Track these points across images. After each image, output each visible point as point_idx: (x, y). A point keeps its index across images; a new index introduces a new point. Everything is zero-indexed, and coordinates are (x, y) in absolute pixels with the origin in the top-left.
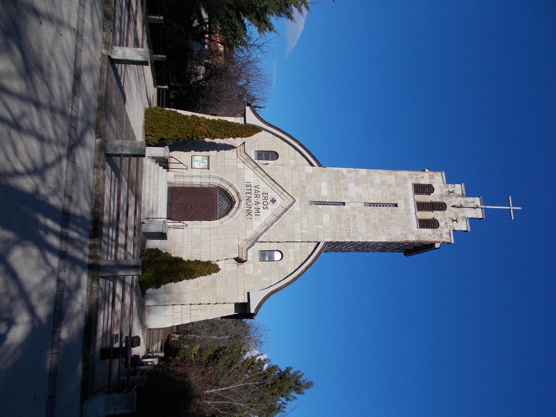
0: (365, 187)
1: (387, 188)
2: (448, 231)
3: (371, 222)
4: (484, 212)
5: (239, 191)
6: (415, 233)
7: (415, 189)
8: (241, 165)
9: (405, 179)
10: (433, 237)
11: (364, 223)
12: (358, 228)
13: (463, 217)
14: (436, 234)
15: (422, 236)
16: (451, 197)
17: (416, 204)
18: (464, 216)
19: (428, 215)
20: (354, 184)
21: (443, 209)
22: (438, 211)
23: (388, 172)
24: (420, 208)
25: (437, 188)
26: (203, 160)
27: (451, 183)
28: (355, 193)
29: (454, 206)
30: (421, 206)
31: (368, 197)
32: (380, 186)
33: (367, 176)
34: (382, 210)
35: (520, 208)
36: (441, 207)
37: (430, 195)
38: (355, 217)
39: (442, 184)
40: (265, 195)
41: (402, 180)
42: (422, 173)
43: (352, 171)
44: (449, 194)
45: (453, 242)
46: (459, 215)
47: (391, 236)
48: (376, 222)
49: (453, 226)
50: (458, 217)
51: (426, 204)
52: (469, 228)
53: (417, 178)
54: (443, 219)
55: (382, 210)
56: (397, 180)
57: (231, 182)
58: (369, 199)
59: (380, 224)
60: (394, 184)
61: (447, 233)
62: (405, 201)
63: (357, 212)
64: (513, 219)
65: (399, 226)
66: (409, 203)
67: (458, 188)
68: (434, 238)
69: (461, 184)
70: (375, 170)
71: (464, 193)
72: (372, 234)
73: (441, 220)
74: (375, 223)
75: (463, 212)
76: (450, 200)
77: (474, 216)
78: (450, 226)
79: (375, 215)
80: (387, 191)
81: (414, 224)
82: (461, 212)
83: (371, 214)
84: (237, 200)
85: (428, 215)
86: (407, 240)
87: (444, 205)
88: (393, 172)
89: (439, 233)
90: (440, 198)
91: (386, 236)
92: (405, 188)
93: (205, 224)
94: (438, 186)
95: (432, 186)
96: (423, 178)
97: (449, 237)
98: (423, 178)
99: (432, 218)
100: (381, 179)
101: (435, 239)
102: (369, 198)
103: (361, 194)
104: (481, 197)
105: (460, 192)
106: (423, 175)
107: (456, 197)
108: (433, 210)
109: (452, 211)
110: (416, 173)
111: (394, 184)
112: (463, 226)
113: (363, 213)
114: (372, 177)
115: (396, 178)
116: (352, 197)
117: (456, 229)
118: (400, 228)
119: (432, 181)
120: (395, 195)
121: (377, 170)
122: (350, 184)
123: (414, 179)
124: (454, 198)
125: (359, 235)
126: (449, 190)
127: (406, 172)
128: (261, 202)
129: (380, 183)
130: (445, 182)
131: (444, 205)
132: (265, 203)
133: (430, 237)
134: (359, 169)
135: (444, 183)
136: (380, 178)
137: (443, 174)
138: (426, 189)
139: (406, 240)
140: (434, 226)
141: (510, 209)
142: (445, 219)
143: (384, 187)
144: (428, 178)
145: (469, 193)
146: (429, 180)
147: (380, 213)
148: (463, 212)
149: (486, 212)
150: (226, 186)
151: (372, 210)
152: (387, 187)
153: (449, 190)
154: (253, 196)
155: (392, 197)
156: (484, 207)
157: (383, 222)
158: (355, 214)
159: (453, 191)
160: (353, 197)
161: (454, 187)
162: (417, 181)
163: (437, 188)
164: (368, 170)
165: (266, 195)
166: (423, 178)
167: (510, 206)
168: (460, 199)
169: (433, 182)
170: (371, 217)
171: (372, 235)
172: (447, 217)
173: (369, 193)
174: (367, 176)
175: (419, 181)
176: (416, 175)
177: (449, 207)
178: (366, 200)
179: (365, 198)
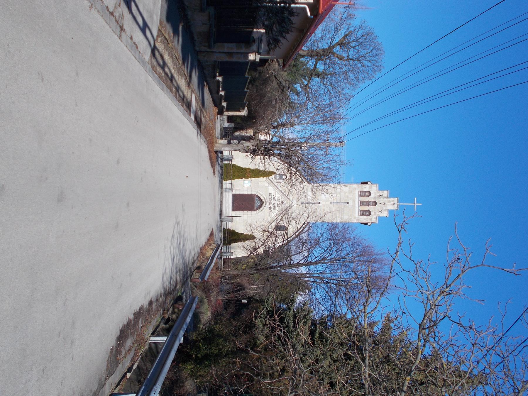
5: (266, 198)
8: (267, 185)
9: (355, 189)
15: (360, 220)
16: (381, 198)
26: (248, 182)
30: (362, 203)
36: (374, 203)
39: (376, 191)
40: (278, 200)
45: (377, 223)
57: (262, 194)
61: (375, 218)
67: (385, 193)
71: (389, 196)
73: (373, 211)
76: (379, 200)
77: (392, 209)
78: (377, 214)
81: (357, 213)
84: (264, 202)
89: (370, 218)
90: (374, 199)
93: (249, 213)
98: (365, 188)
105: (386, 196)
112: (384, 214)
115: (349, 188)
117: (381, 216)
119: (370, 189)
124: (382, 199)
128: (276, 203)
130: (378, 190)
132: (278, 204)
137: (378, 185)
142: (375, 210)
145: (391, 196)
149: (399, 206)
150: (259, 195)
154: (272, 200)
161: (383, 193)
165: (279, 200)
166: (365, 188)
168: (385, 199)
176: (361, 186)
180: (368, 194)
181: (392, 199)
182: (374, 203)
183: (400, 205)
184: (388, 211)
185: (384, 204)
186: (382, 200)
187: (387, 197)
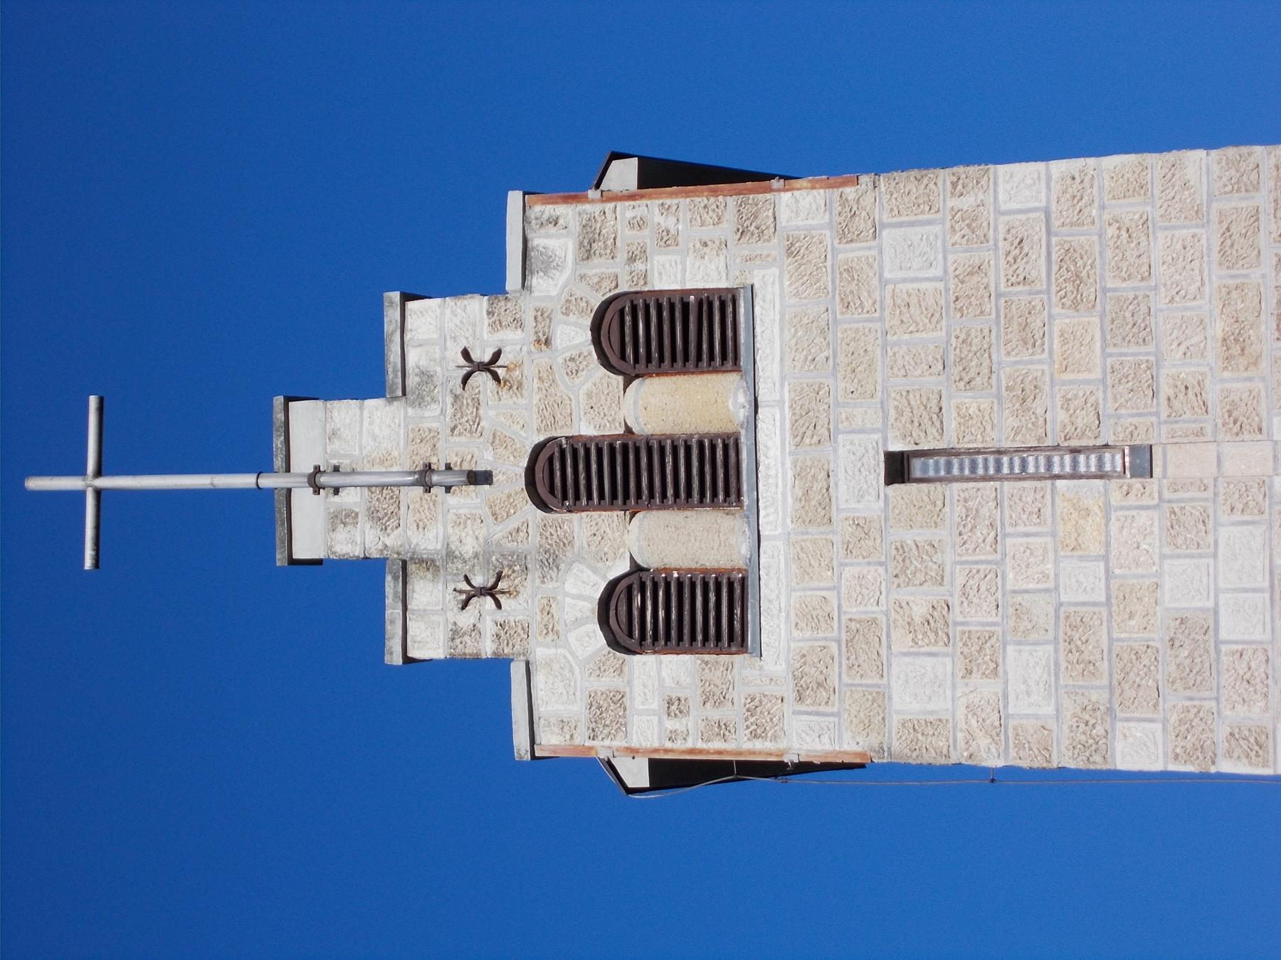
0: (1131, 616)
1: (956, 609)
2: (536, 281)
3: (1102, 316)
4: (278, 442)
6: (774, 247)
7: (738, 611)
10: (646, 232)
11: (1160, 301)
12: (1215, 256)
13: (420, 402)
14: (622, 256)
17: (745, 488)
18: (410, 411)
20: (1223, 635)
21: (551, 460)
22: (586, 442)
23: (942, 744)
24: (720, 452)
25: (578, 622)
27: (475, 664)
28: (1215, 556)
29: (479, 478)
31: (1114, 527)
32: (1012, 623)
33: (1110, 710)
34: (1012, 422)
35: (35, 484)
37: (637, 569)
38: (1236, 350)
41: (834, 681)
42: (679, 745)
43: (1229, 754)
44: (499, 577)
45: (514, 199)
46: (450, 411)
47: (953, 210)
48: (1063, 320)
49: (496, 325)
50: (456, 397)
51: (670, 492)
52: (392, 316)
53: (718, 704)
54: (560, 373)
55: (1012, 422)
56: (876, 681)
58: (1107, 510)
59: (1037, 302)
60: (895, 649)
61: (549, 265)
62: (826, 502)
63: (1213, 394)
64: (93, 401)
65: (888, 301)
66: (799, 493)
68: (640, 224)
69: (408, 660)
70: (1039, 763)
71: (391, 587)
72: (1106, 217)
74: (1075, 306)
75: (420, 437)
76: (499, 532)
77: (344, 411)
78: (519, 323)
79: (1068, 376)
80: (960, 580)
82: (432, 439)
83: (1104, 381)
86: (836, 192)
87: (543, 490)
88: (896, 747)
89: (599, 267)
90: (567, 542)
91: (998, 212)
92: (810, 617)
94: (572, 637)
95: (614, 643)
96: (670, 703)
97: (537, 241)
98: (674, 706)
99: (636, 383)
100: (987, 689)
101: (629, 214)
102: (1108, 520)
103: (1167, 551)
104: (280, 559)
106: (671, 724)
107: (450, 555)
108: (625, 447)
109: (496, 440)
110: (717, 745)
111: (901, 641)
113: (1165, 390)
114: (1067, 703)
115: (880, 698)
116: (1247, 518)
117: (476, 305)
118: (883, 283)
119: (608, 682)
120: (901, 548)
121: (1025, 764)
122: (1257, 636)
123: (739, 695)
124: (469, 547)
125: (1210, 200)
126: (499, 605)
127: (796, 745)
129: (1010, 649)
131: (543, 490)
133: (670, 222)
134: (1173, 767)
135: (527, 663)
136: (1006, 696)
138: (661, 614)
139: (850, 191)
140: (628, 319)
141: (99, 473)
143: (978, 615)
144: (638, 704)
146: (629, 683)
147: (1025, 395)
148: (420, 437)
151: (1092, 418)
152: (956, 615)
153: (499, 605)
155: (923, 535)
156: (267, 482)
157: (1010, 321)
158: (1226, 374)
159: (465, 605)
160: (1237, 517)
162: (716, 675)
163: (578, 622)
164: (1098, 764)
166: (674, 706)
167: (99, 493)
168: (428, 542)
169: (600, 670)
170: (1105, 355)
171: (1103, 207)
172: (532, 395)
173: (1106, 558)
174: (1110, 710)
175: (708, 675)
176: (723, 729)
177: (511, 473)
178: (1132, 500)
179: (1143, 518)
183: (263, 467)
184: (393, 375)
185: (424, 477)
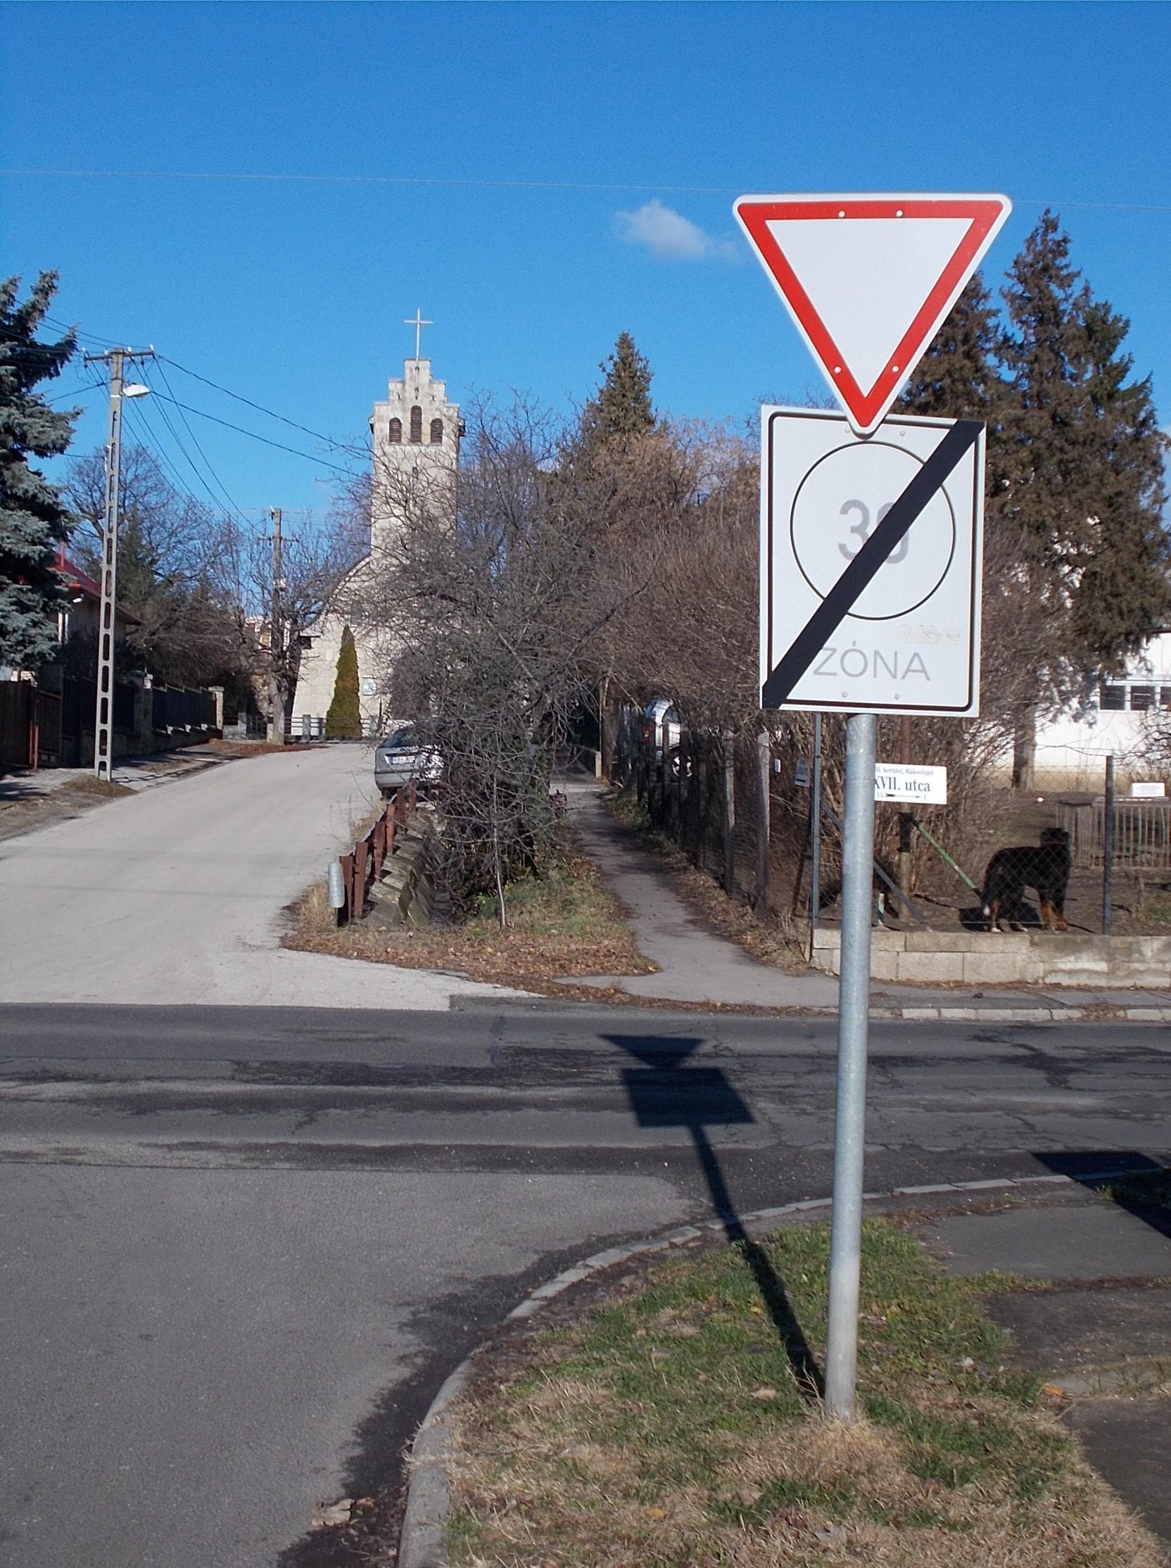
13: (429, 386)
16: (404, 397)
19: (426, 429)
30: (416, 438)
36: (416, 411)
67: (394, 387)
73: (433, 415)
76: (408, 400)
77: (428, 371)
85: (426, 429)
105: (399, 386)
112: (440, 389)
137: (376, 403)
142: (431, 410)
166: (381, 430)
168: (407, 387)
180: (396, 423)
181: (407, 371)
182: (416, 411)
186: (410, 393)
187: (403, 382)
